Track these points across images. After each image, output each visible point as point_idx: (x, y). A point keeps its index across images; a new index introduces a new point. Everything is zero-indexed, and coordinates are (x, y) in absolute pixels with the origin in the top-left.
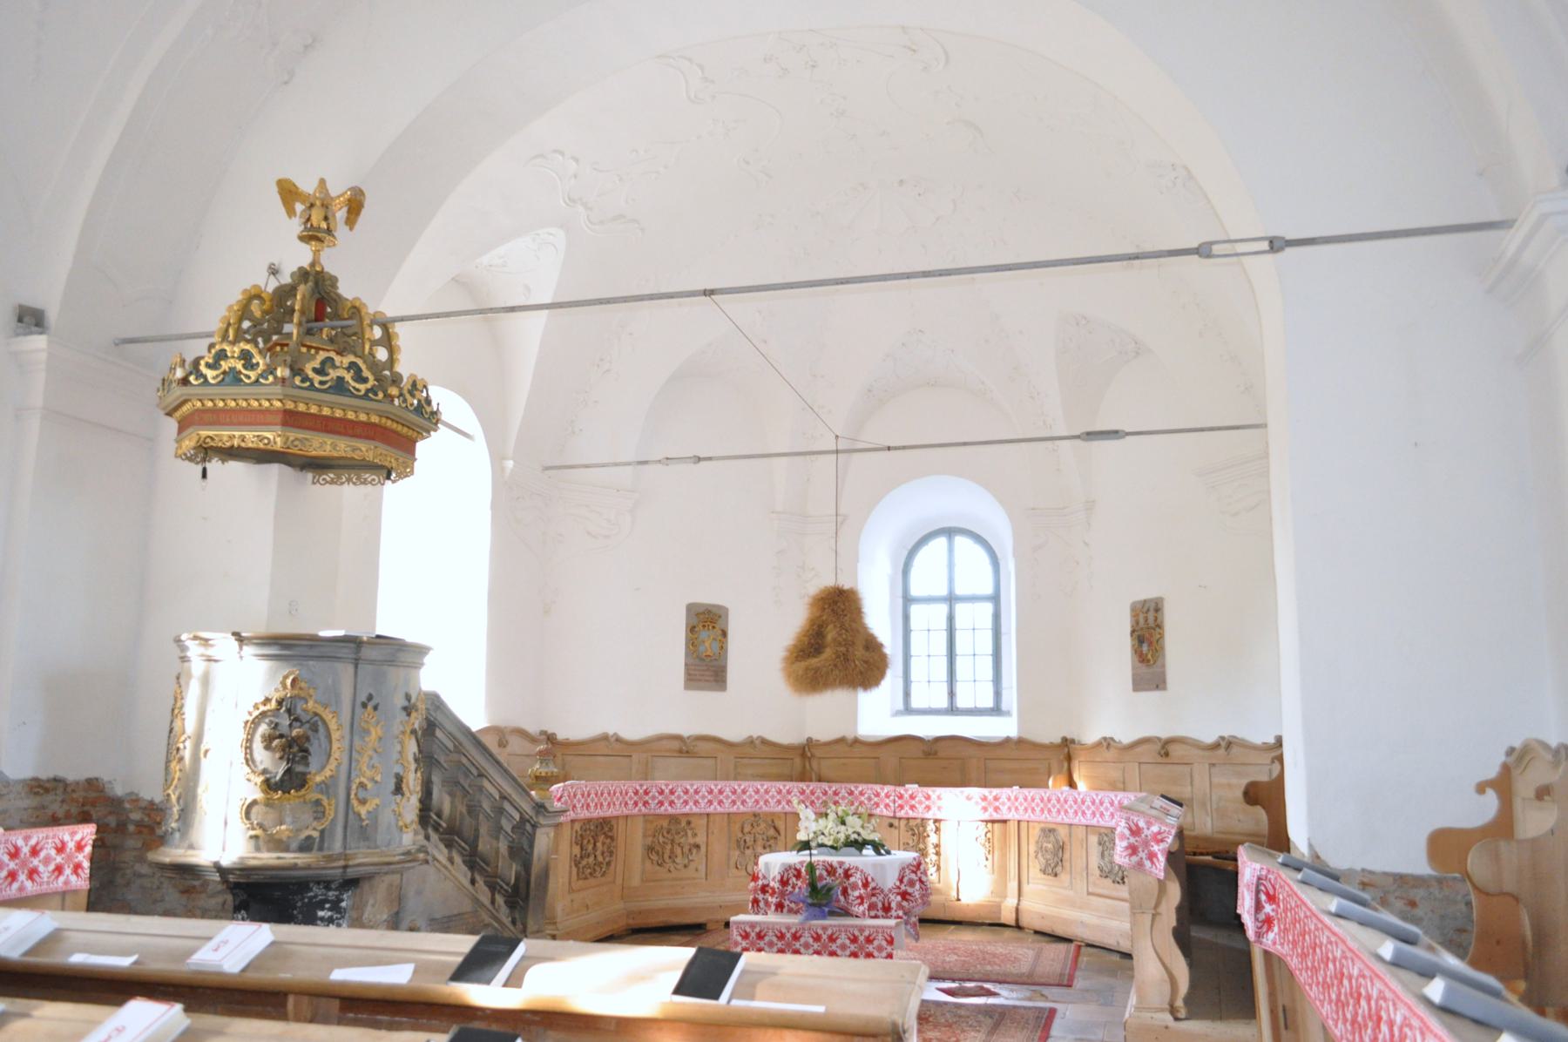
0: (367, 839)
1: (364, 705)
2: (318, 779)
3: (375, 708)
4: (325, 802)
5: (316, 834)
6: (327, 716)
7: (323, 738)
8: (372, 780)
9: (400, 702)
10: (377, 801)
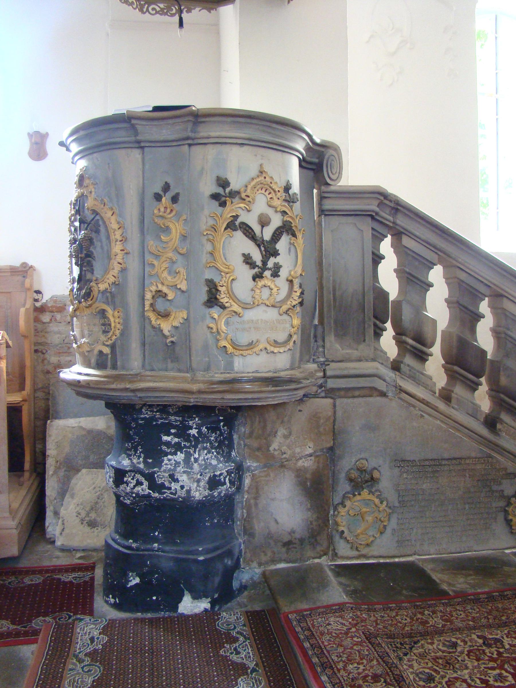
0: (175, 359)
1: (158, 197)
2: (102, 287)
3: (175, 199)
4: (110, 312)
5: (106, 350)
7: (104, 239)
8: (174, 287)
9: (209, 187)
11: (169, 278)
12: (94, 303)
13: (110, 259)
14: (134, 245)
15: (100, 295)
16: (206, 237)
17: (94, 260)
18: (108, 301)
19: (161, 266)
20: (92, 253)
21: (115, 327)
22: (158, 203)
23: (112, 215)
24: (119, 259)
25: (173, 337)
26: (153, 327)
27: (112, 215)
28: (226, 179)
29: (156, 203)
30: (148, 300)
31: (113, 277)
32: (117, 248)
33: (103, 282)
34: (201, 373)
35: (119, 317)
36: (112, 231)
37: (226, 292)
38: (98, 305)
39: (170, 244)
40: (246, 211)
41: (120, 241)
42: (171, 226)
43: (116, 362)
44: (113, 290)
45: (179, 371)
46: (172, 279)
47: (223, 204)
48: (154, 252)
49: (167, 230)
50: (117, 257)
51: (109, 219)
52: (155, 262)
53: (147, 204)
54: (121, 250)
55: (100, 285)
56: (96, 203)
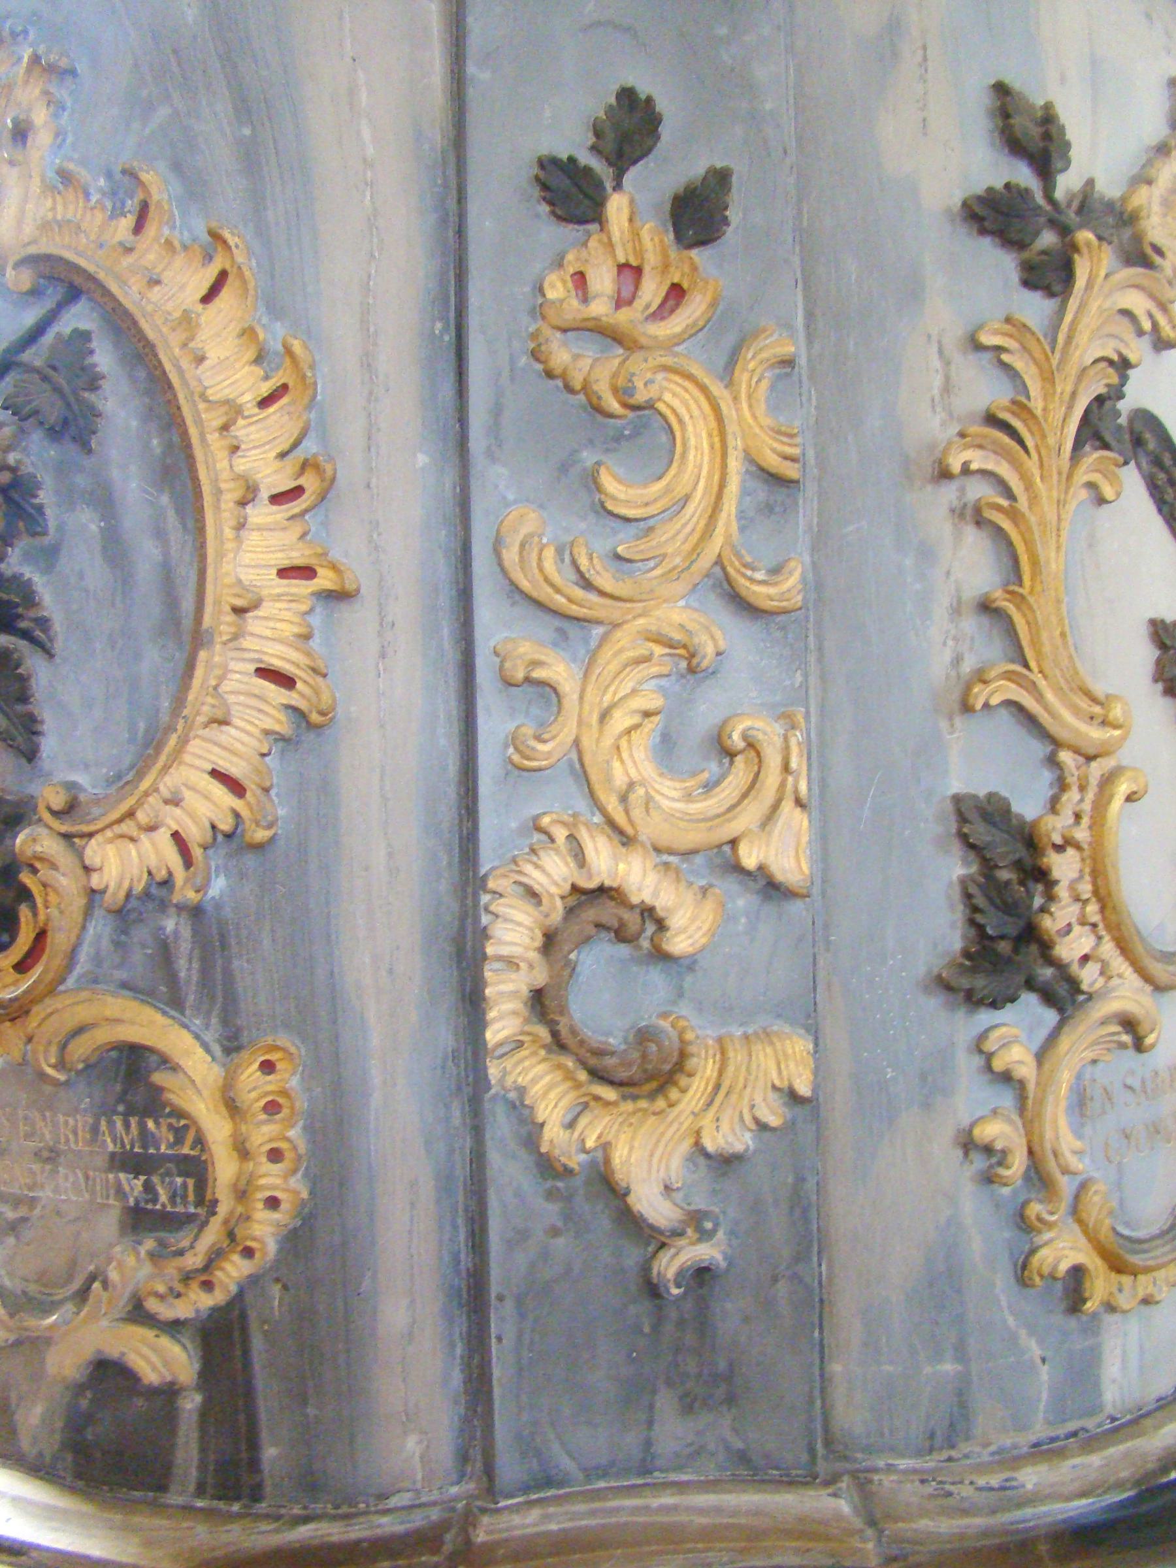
0: (717, 1387)
1: (570, 193)
2: (119, 864)
3: (697, 215)
4: (194, 1070)
5: (164, 1360)
6: (165, 287)
7: (131, 482)
10: (791, 1061)
11: (668, 793)
12: (52, 989)
13: (199, 639)
14: (389, 529)
15: (100, 928)
16: (948, 493)
17: (49, 654)
18: (172, 980)
19: (613, 709)
20: (29, 598)
21: (242, 1194)
22: (571, 231)
23: (207, 299)
24: (273, 634)
25: (705, 1235)
26: (547, 1167)
27: (207, 299)
28: (1048, 107)
29: (554, 235)
30: (511, 963)
31: (219, 791)
32: (251, 552)
33: (127, 827)
34: (903, 1463)
35: (272, 1108)
36: (213, 420)
37: (1086, 889)
38: (83, 1013)
39: (673, 539)
40: (1145, 343)
41: (276, 499)
42: (676, 398)
43: (254, 1445)
44: (218, 886)
45: (750, 1468)
46: (688, 797)
47: (1050, 275)
48: (545, 593)
49: (638, 427)
50: (253, 623)
51: (187, 321)
52: (559, 670)
53: (483, 226)
54: (283, 573)
55: (94, 851)
56: (69, 208)
